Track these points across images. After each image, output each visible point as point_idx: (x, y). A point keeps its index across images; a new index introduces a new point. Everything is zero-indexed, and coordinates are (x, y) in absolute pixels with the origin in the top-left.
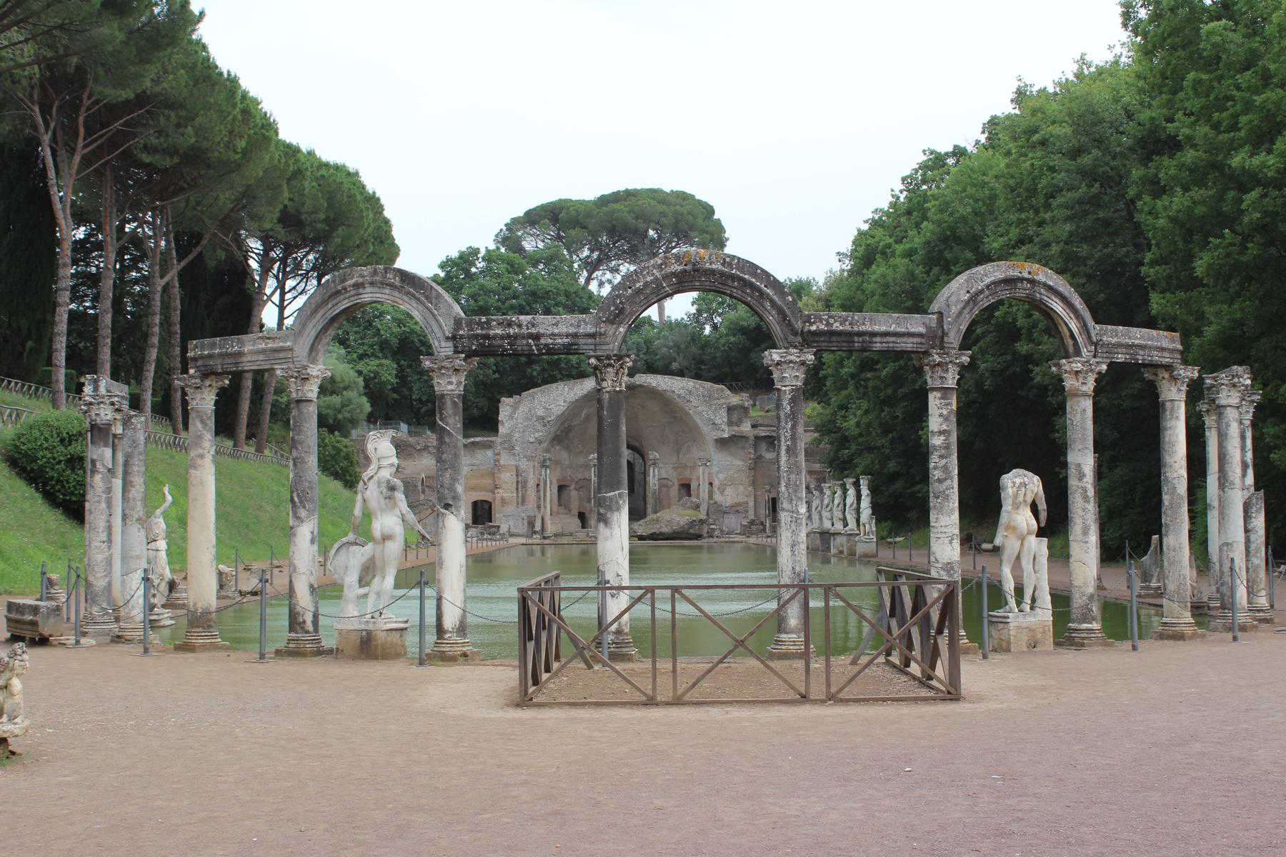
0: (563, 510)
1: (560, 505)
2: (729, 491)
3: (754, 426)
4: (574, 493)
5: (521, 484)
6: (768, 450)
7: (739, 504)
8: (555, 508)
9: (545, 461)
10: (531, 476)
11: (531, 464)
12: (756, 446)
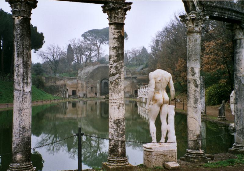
0: (92, 92)
1: (91, 91)
2: (127, 88)
3: (132, 75)
4: (94, 89)
5: (83, 87)
6: (135, 80)
7: (128, 91)
8: (90, 92)
9: (87, 82)
10: (85, 85)
11: (85, 83)
12: (132, 79)
